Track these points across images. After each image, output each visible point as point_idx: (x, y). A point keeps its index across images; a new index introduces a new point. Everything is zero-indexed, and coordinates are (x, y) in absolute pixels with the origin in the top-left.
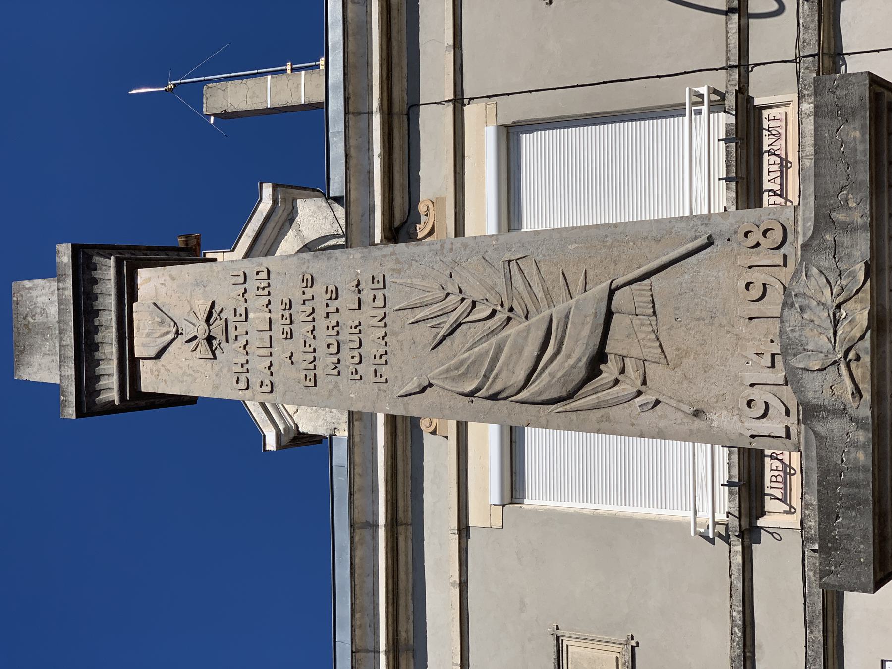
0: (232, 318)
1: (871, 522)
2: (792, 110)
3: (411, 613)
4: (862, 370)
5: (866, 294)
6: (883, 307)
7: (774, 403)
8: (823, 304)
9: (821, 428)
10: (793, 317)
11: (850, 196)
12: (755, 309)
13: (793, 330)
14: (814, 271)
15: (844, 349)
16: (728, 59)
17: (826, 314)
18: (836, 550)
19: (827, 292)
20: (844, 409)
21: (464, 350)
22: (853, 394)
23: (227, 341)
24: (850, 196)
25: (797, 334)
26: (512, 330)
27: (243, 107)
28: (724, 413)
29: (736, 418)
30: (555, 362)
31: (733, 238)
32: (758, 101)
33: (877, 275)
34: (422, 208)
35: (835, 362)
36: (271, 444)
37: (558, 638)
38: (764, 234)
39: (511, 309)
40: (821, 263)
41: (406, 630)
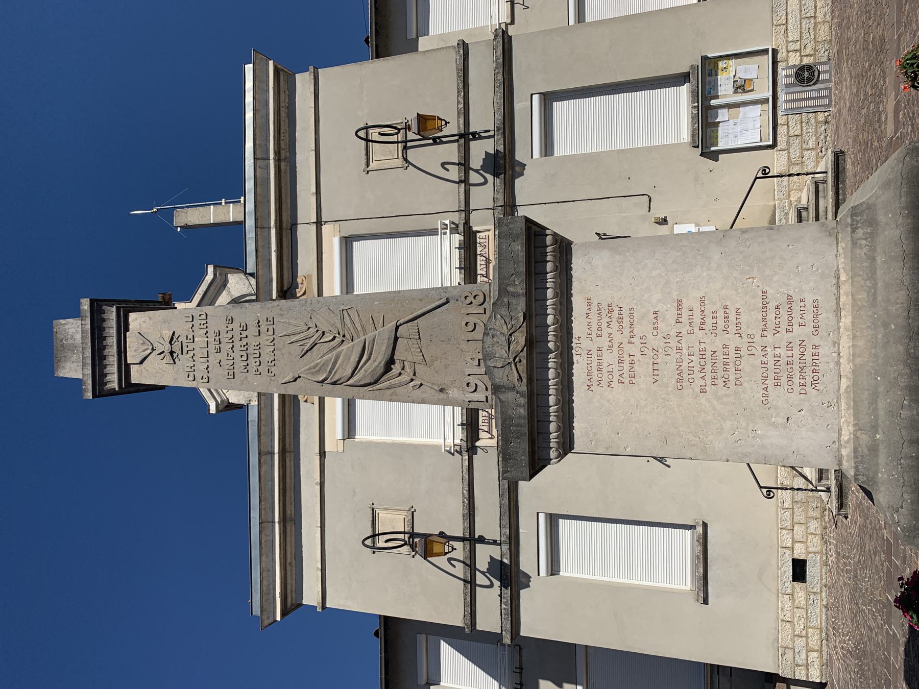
0: (185, 341)
1: (527, 444)
2: (491, 234)
3: (293, 500)
4: (522, 367)
5: (524, 329)
6: (532, 335)
7: (480, 384)
8: (503, 334)
9: (502, 397)
10: (488, 340)
11: (516, 279)
12: (470, 336)
13: (488, 347)
14: (499, 316)
15: (514, 357)
16: (459, 207)
17: (505, 339)
18: (510, 459)
19: (505, 327)
20: (514, 387)
21: (318, 358)
22: (518, 379)
23: (182, 354)
24: (516, 279)
25: (490, 349)
26: (344, 347)
27: (197, 222)
28: (456, 389)
29: (461, 392)
30: (368, 364)
31: (459, 300)
32: (474, 229)
33: (529, 319)
34: (299, 280)
35: (509, 363)
36: (213, 410)
37: (373, 509)
38: (475, 297)
39: (344, 336)
40: (502, 313)
41: (290, 510)
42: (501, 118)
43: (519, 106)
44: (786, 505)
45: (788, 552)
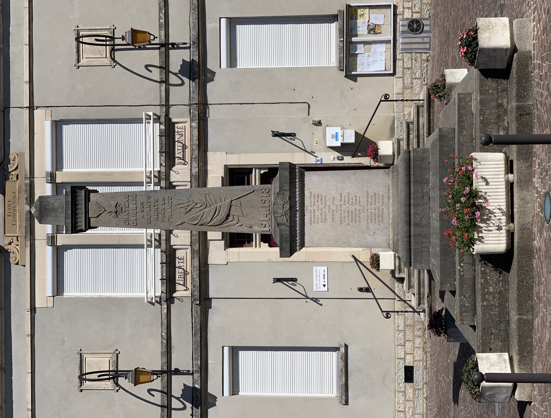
2: (187, 125)
32: (173, 120)
34: (11, 157)
42: (196, 34)
43: (210, 26)
44: (400, 328)
45: (402, 362)
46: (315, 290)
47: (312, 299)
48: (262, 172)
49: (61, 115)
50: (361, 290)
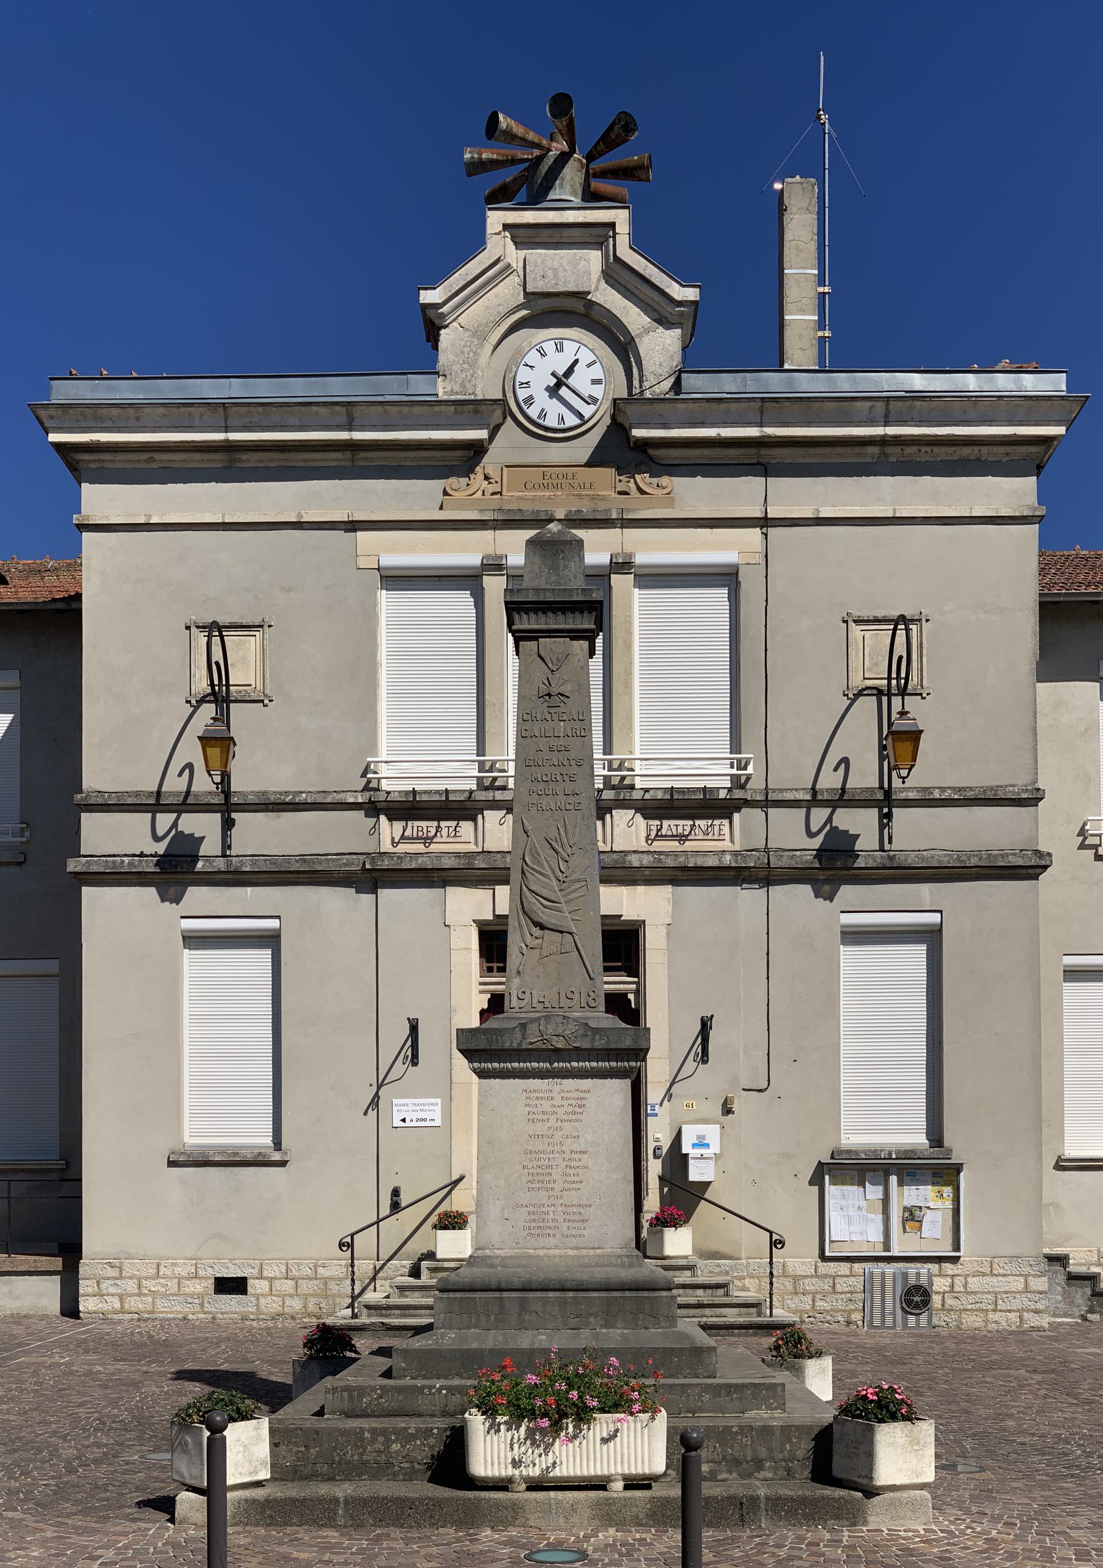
2: (726, 845)
34: (665, 480)
42: (909, 862)
44: (320, 1270)
45: (255, 1272)
46: (395, 1101)
47: (377, 1095)
48: (631, 997)
49: (751, 584)
50: (396, 1192)
